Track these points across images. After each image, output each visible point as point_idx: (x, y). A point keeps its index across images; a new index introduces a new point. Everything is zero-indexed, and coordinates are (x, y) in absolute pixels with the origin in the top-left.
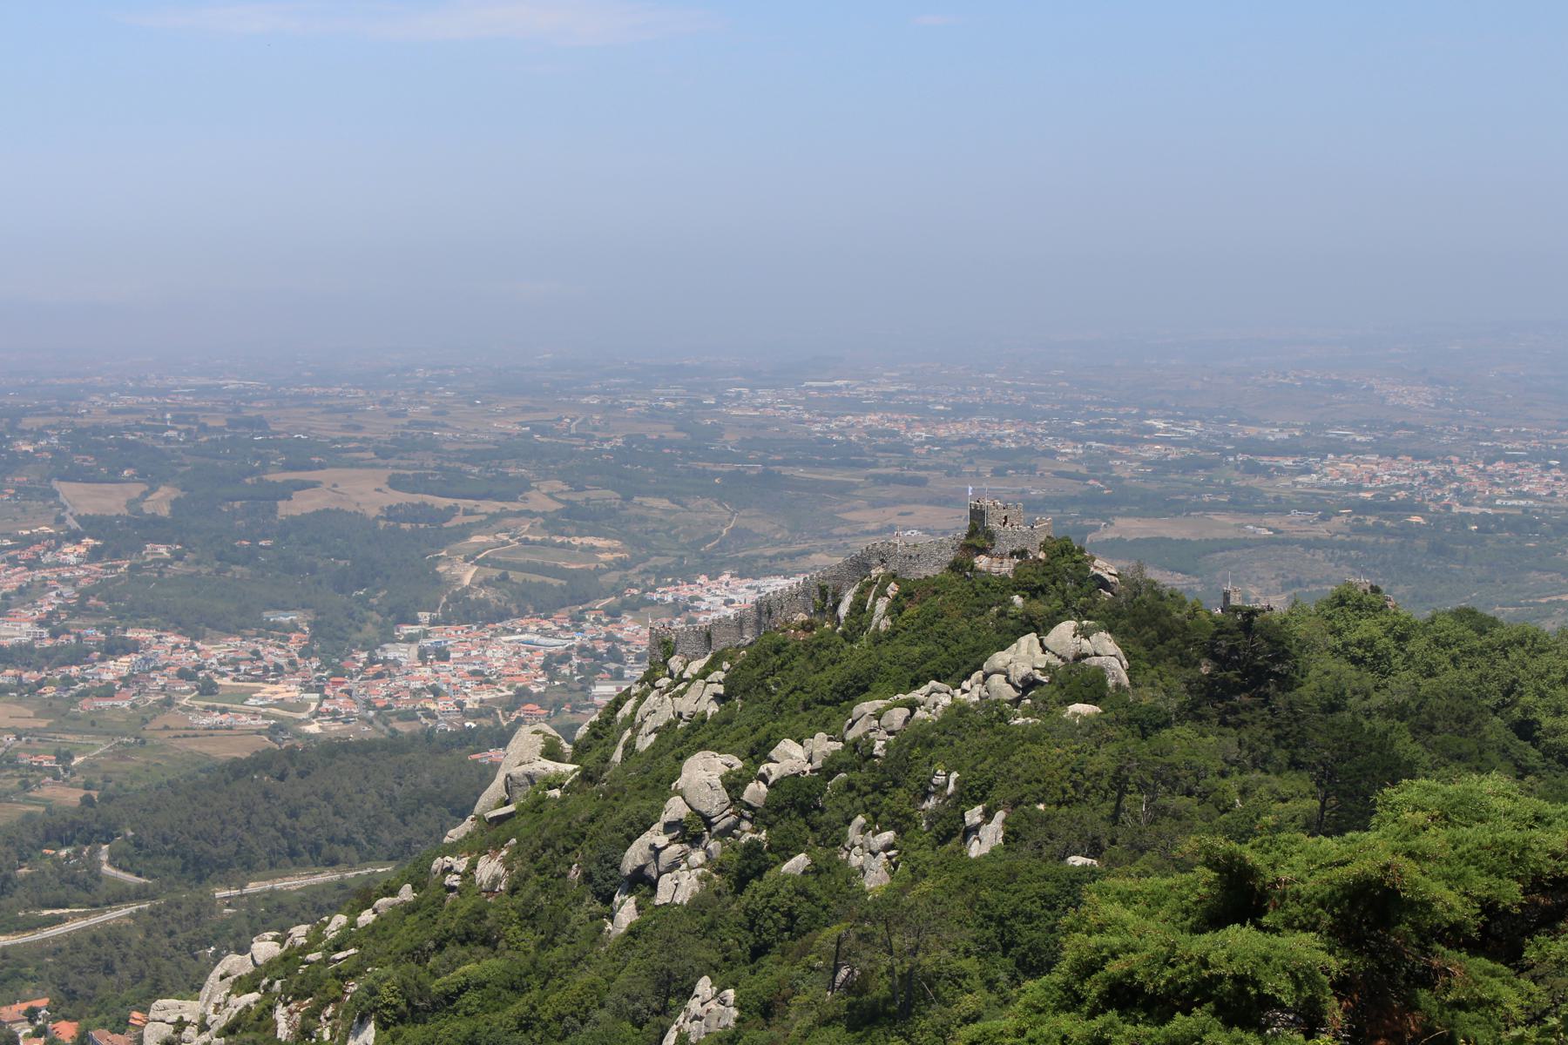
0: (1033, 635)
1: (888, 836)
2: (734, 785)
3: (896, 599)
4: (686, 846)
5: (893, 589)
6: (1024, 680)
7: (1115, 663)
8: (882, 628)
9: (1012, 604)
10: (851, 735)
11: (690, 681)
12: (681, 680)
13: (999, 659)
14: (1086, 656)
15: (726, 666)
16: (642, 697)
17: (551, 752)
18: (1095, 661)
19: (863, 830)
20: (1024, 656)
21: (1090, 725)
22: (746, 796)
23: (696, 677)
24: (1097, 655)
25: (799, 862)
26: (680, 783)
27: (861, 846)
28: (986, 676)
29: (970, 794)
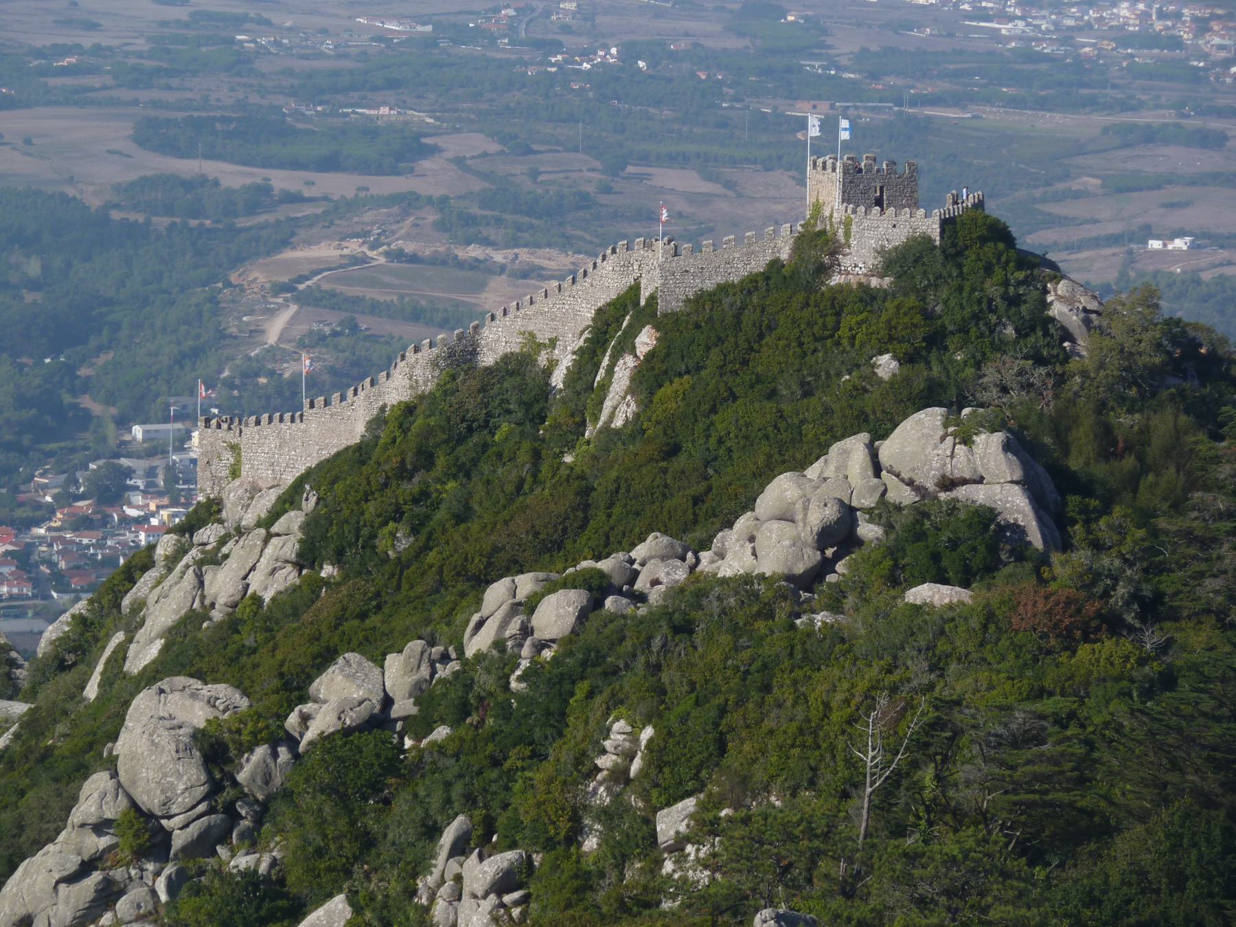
0: (864, 437)
2: (215, 751)
3: (650, 356)
5: (646, 340)
8: (618, 423)
13: (782, 489)
18: (979, 495)
19: (460, 849)
23: (259, 524)
24: (980, 481)
26: (121, 747)
29: (668, 776)
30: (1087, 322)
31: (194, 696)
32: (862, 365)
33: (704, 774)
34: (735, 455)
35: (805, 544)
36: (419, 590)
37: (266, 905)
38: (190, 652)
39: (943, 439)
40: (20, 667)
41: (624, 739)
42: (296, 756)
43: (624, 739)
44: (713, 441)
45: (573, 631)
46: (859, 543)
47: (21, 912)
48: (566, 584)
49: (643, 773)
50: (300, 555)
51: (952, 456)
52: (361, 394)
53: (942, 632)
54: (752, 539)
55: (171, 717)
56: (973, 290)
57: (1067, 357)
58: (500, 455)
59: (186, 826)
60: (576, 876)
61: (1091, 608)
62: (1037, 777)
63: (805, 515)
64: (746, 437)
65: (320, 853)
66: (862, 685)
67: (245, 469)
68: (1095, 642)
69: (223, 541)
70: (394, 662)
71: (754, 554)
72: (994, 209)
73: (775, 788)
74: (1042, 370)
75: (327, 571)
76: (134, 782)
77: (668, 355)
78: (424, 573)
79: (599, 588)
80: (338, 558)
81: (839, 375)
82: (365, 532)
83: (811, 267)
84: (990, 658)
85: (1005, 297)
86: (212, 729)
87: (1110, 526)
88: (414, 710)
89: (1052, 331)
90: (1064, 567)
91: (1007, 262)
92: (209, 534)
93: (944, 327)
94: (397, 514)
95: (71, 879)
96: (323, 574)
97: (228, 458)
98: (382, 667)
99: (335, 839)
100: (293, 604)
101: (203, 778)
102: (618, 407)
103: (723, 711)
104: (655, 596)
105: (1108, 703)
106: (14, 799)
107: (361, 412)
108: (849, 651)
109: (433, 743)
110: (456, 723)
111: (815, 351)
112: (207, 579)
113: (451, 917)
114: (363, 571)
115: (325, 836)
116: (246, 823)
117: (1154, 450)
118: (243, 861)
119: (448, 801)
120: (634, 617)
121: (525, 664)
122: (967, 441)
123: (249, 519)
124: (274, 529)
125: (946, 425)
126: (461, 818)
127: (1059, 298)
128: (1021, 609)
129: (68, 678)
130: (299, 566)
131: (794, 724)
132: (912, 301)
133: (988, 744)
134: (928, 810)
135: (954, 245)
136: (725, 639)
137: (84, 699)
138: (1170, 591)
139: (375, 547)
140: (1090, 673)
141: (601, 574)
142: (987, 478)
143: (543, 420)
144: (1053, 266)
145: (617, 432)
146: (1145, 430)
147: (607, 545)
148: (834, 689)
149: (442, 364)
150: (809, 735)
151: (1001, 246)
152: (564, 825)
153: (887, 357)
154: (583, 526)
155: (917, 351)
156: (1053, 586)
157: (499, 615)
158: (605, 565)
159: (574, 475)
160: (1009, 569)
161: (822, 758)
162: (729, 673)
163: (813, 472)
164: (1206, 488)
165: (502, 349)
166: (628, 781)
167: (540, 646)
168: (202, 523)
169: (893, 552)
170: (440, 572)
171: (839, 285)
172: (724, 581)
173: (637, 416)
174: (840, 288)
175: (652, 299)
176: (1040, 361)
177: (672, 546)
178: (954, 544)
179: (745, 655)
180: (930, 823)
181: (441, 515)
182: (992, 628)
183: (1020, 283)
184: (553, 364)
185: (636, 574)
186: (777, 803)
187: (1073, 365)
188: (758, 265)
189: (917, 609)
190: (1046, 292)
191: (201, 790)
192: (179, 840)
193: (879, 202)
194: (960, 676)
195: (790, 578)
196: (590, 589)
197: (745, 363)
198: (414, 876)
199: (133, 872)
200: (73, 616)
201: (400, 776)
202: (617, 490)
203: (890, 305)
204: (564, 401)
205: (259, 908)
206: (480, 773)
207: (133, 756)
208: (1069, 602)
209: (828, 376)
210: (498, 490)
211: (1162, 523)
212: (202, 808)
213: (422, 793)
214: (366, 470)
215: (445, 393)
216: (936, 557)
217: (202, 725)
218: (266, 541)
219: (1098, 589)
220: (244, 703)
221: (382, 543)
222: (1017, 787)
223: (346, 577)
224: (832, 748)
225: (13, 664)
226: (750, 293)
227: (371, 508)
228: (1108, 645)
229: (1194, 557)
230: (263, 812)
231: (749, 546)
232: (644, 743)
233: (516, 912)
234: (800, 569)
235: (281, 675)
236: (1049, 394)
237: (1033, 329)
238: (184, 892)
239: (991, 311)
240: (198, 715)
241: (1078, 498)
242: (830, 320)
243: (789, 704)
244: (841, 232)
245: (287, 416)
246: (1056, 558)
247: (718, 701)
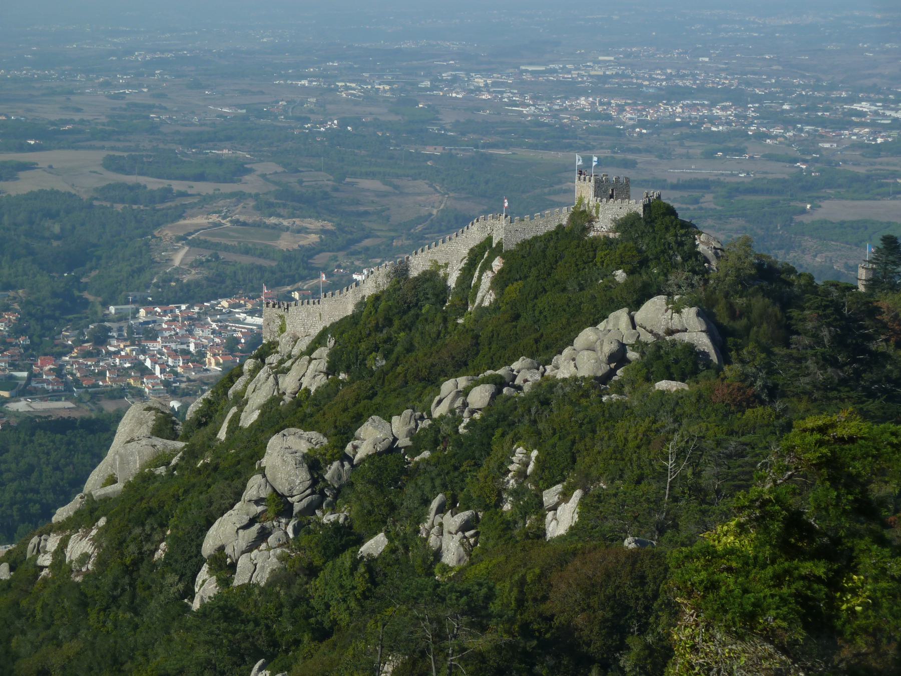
0: (626, 310)
2: (314, 464)
3: (501, 272)
5: (497, 264)
8: (486, 304)
10: (437, 413)
12: (289, 357)
13: (587, 335)
16: (254, 372)
18: (686, 337)
19: (441, 510)
23: (302, 354)
24: (685, 330)
25: (375, 545)
26: (265, 461)
29: (548, 473)
30: (716, 254)
31: (300, 437)
32: (608, 275)
33: (565, 473)
34: (549, 320)
35: (602, 362)
36: (394, 385)
37: (344, 539)
39: (666, 311)
40: (178, 424)
41: (523, 457)
42: (352, 466)
43: (523, 457)
44: (537, 313)
45: (489, 404)
46: (629, 361)
47: (219, 543)
48: (485, 381)
49: (534, 472)
50: (327, 369)
51: (671, 319)
52: (350, 291)
53: (677, 403)
54: (574, 359)
55: (290, 448)
56: (661, 239)
57: (707, 271)
58: (426, 320)
59: (301, 500)
60: (502, 523)
61: (750, 392)
62: (744, 473)
63: (602, 348)
64: (554, 310)
65: (370, 513)
66: (641, 430)
67: (289, 328)
68: (754, 407)
69: (281, 362)
70: (395, 419)
71: (575, 366)
72: (664, 199)
73: (603, 479)
74: (696, 278)
75: (342, 376)
76: (274, 480)
77: (510, 271)
78: (396, 377)
79: (500, 383)
80: (347, 370)
81: (597, 280)
82: (361, 357)
83: (580, 228)
84: (703, 416)
85: (676, 242)
86: (312, 454)
87: (749, 353)
88: (410, 443)
89: (699, 258)
90: (731, 371)
91: (676, 225)
92: (273, 359)
93: (647, 256)
94: (376, 349)
95: (245, 527)
96: (340, 378)
97: (278, 322)
98: (390, 422)
99: (378, 506)
100: (327, 393)
101: (309, 477)
102: (486, 296)
103: (573, 442)
104: (527, 388)
105: (765, 438)
106: (205, 488)
107: (350, 299)
108: (632, 413)
109: (423, 460)
110: (433, 449)
111: (584, 268)
113: (439, 543)
114: (361, 378)
115: (372, 504)
116: (329, 499)
117: (755, 314)
118: (329, 518)
119: (434, 487)
120: (520, 398)
121: (467, 420)
122: (678, 311)
123: (296, 351)
124: (313, 356)
125: (667, 304)
126: (440, 495)
127: (702, 242)
128: (716, 392)
129: (208, 429)
130: (327, 374)
131: (611, 450)
132: (631, 244)
133: (719, 456)
134: (690, 489)
135: (650, 217)
136: (568, 407)
137: (219, 439)
138: (781, 383)
139: (365, 365)
140: (755, 423)
141: (501, 377)
142: (689, 329)
143: (445, 302)
144: (694, 226)
145: (486, 308)
146: (749, 306)
147: (492, 363)
148: (627, 432)
149: (392, 275)
150: (618, 453)
151: (673, 217)
152: (494, 499)
153: (620, 271)
154: (477, 354)
155: (635, 268)
156: (726, 382)
157: (450, 397)
158: (501, 372)
159: (466, 330)
160: (704, 373)
161: (626, 464)
162: (573, 424)
163: (601, 326)
164: (798, 334)
165: (421, 269)
166: (526, 477)
167: (472, 412)
168: (268, 354)
169: (647, 365)
170: (405, 376)
171: (594, 237)
172: (564, 380)
173: (496, 300)
174: (595, 238)
175: (500, 244)
176: (695, 272)
177: (532, 363)
178: (676, 361)
179: (581, 415)
180: (690, 496)
181: (399, 349)
182: (702, 401)
183: (682, 236)
184: (446, 276)
185: (515, 377)
186: (604, 487)
187: (713, 275)
188: (552, 227)
189: (662, 393)
190: (695, 239)
191: (308, 483)
192: (297, 507)
193: (611, 196)
194: (689, 425)
195: (596, 378)
196: (496, 384)
197: (549, 274)
198: (418, 523)
199: (275, 523)
200: (204, 400)
201: (407, 475)
202: (493, 336)
203: (621, 246)
204: (456, 293)
205: (341, 540)
206: (448, 473)
207: (274, 467)
208: (739, 389)
209: (591, 281)
210: (427, 337)
211: (776, 350)
212: (308, 491)
213: (420, 484)
214: (359, 327)
215: (395, 290)
216: (668, 367)
217: (306, 451)
218: (310, 362)
219: (747, 383)
220: (325, 441)
221: (368, 363)
222: (734, 477)
223: (352, 381)
224: (631, 460)
225: (174, 423)
226: (549, 241)
227: (363, 346)
228: (760, 410)
229: (791, 367)
230: (338, 493)
231: (572, 363)
232: (533, 459)
233: (472, 541)
234: (600, 374)
235: (336, 427)
236: (701, 289)
237: (690, 257)
238: (302, 533)
239: (671, 249)
240: (303, 447)
241: (731, 339)
242: (591, 254)
243: (606, 438)
244: (594, 211)
245: (311, 301)
246: (726, 368)
247: (571, 437)
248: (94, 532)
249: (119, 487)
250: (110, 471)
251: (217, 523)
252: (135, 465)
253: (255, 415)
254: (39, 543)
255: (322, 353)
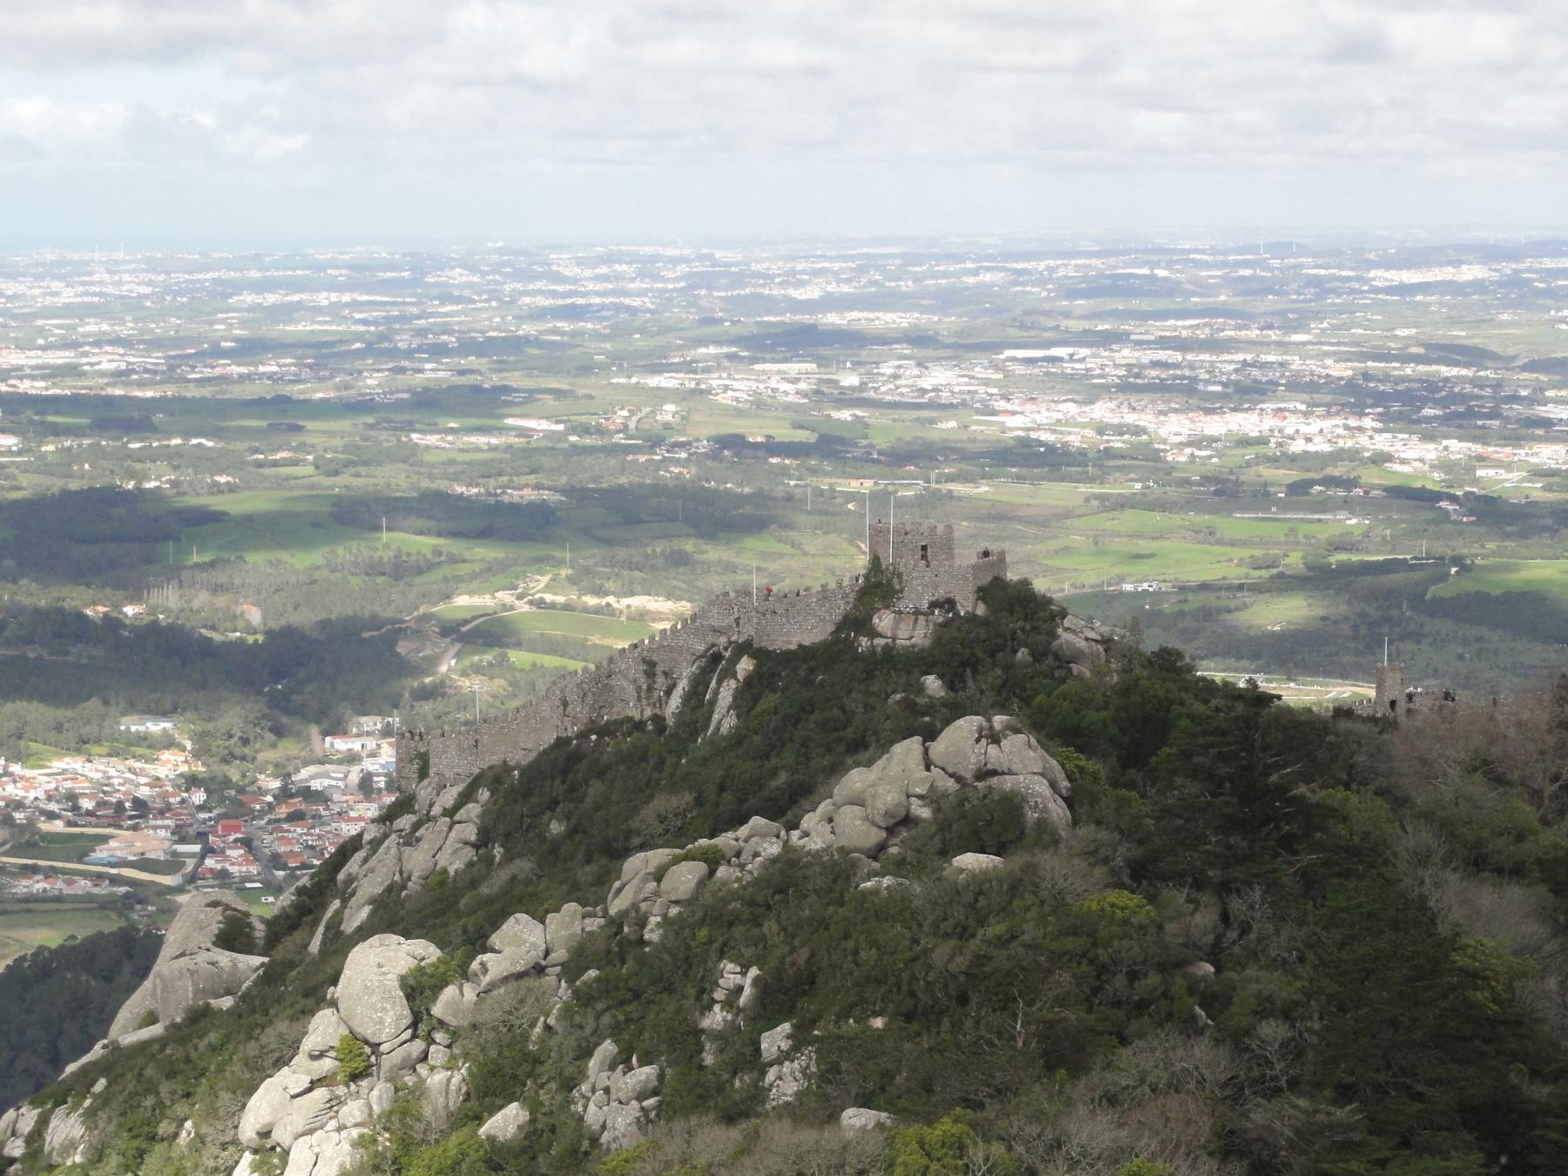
0: (918, 739)
1: (645, 1074)
2: (418, 990)
3: (749, 682)
4: (341, 1090)
5: (745, 666)
6: (887, 814)
7: (1041, 787)
8: (724, 730)
9: (921, 690)
10: (616, 906)
11: (435, 819)
13: (857, 779)
14: (994, 773)
15: (484, 794)
16: (376, 844)
17: (234, 936)
18: (1008, 783)
20: (895, 777)
21: (980, 883)
22: (437, 1010)
24: (1010, 773)
27: (607, 1090)
28: (837, 806)
38: (392, 916)
39: (978, 741)
41: (733, 976)
54: (830, 820)
67: (432, 771)
69: (417, 826)
92: (405, 822)
102: (723, 719)
112: (405, 857)
124: (456, 818)
129: (297, 936)
130: (476, 846)
157: (636, 881)
173: (737, 727)
191: (407, 1021)
212: (407, 1034)
218: (451, 828)
248: (88, 1102)
249: (157, 1030)
250: (149, 1004)
251: (262, 1087)
252: (185, 996)
253: (364, 913)
254: (16, 1121)
255: (472, 810)
